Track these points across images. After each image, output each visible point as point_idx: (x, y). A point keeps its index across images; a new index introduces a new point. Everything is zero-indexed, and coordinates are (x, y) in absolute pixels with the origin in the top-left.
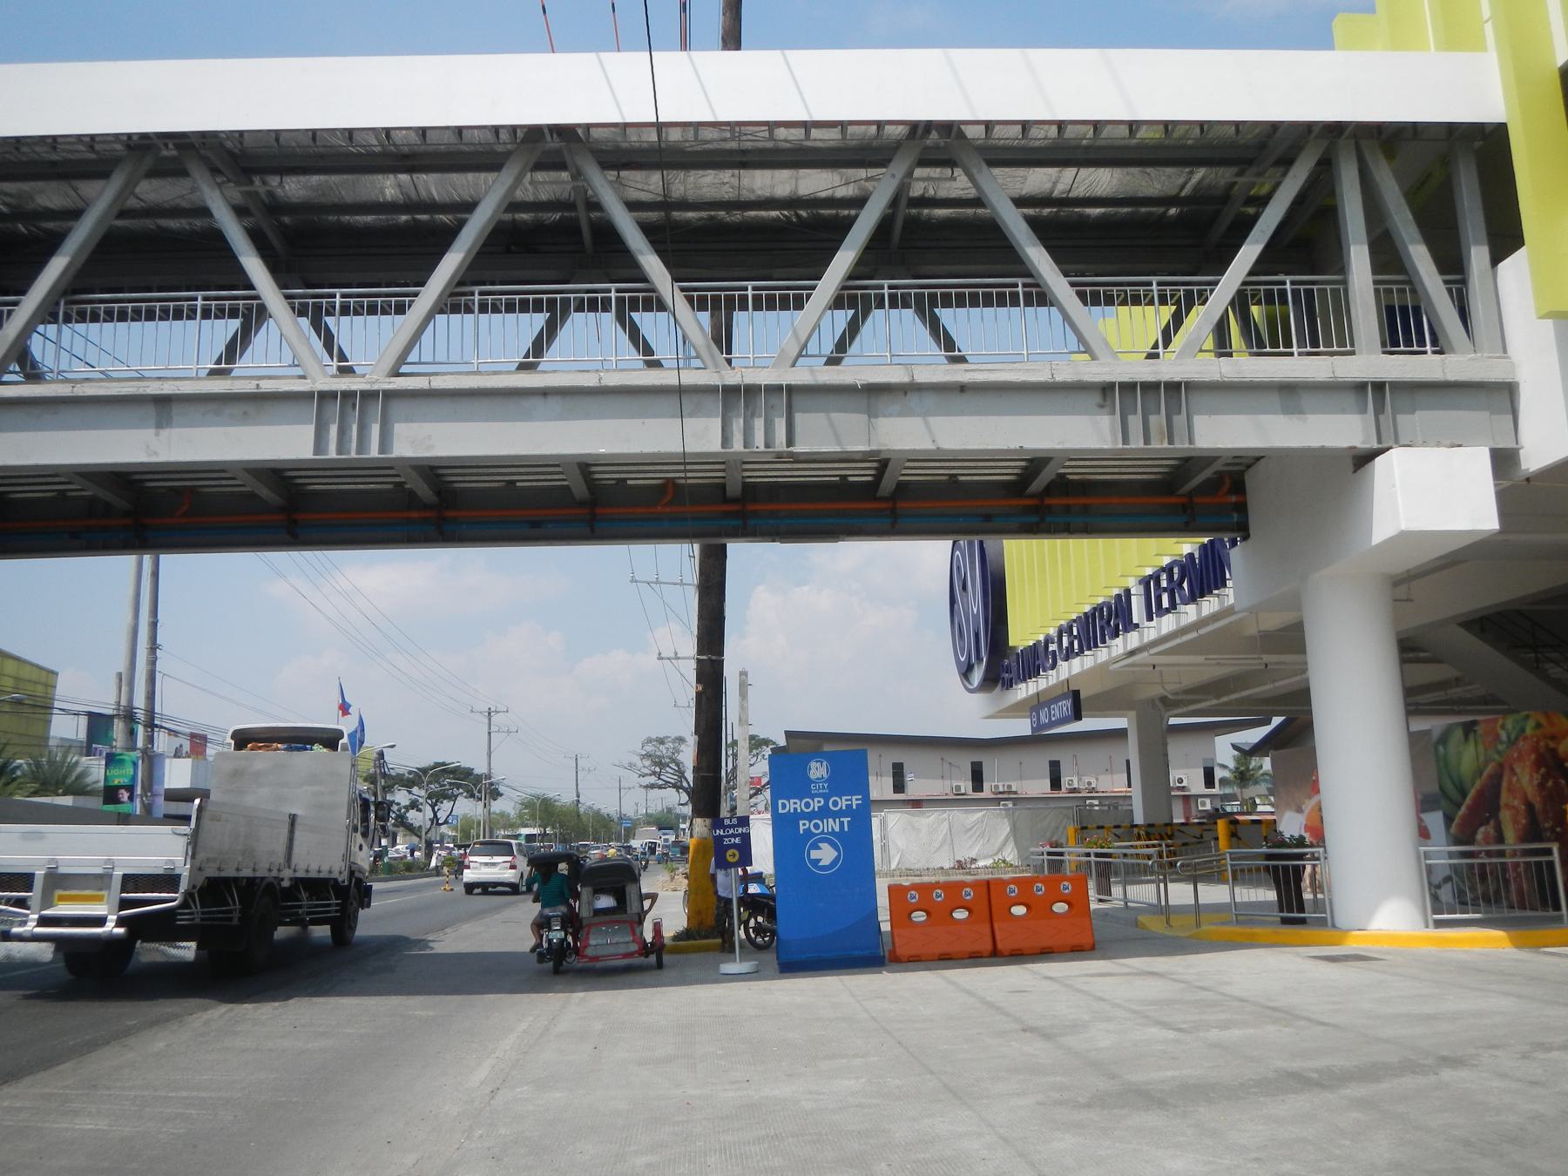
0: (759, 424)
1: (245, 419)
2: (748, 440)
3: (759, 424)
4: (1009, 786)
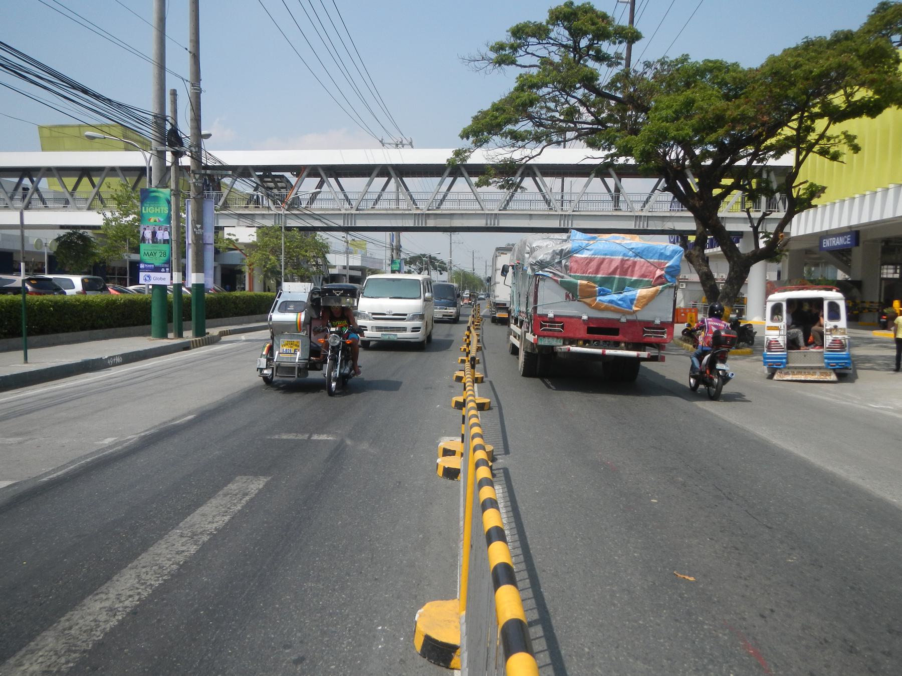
0: (642, 223)
1: (545, 219)
2: (639, 226)
3: (642, 223)
4: (685, 276)
